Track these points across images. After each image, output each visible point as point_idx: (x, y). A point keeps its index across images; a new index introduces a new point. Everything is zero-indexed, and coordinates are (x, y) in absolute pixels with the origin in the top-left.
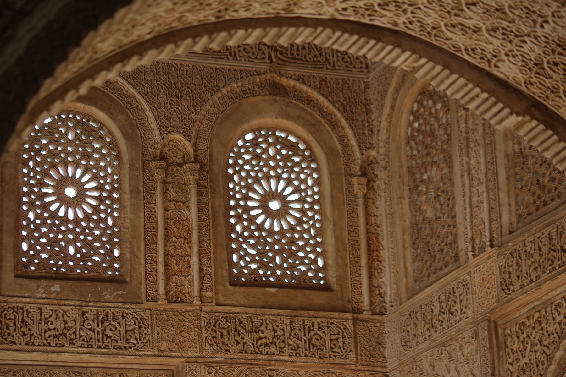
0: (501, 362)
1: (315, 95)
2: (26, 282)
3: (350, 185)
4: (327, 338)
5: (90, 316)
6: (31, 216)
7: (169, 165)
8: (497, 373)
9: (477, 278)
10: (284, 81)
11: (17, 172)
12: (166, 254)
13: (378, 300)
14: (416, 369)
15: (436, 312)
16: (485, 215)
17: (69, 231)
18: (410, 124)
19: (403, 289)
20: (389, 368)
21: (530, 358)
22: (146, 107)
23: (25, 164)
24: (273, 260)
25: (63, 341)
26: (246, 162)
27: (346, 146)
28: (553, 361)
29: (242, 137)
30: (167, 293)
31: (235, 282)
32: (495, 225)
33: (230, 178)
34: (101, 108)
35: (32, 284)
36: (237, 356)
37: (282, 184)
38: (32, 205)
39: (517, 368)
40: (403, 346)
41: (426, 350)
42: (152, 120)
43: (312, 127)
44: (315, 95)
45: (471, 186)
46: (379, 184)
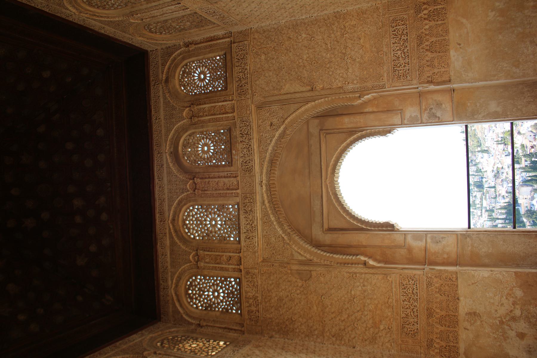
1: (167, 67)
2: (233, 163)
3: (192, 51)
4: (241, 52)
5: (241, 139)
6: (214, 161)
7: (193, 116)
9: (195, 6)
10: (164, 78)
11: (201, 167)
12: (220, 114)
13: (227, 35)
15: (218, 17)
16: (173, 7)
17: (217, 148)
18: (165, 34)
19: (219, 28)
22: (177, 125)
23: (199, 164)
24: (218, 75)
25: (250, 149)
26: (190, 88)
27: (181, 54)
29: (183, 91)
30: (232, 113)
31: (226, 88)
32: (173, 3)
33: (195, 93)
34: (180, 140)
35: (234, 160)
36: (249, 85)
37: (196, 75)
38: (211, 162)
42: (180, 123)
43: (176, 66)
44: (167, 67)
45: (167, 13)
46: (190, 40)
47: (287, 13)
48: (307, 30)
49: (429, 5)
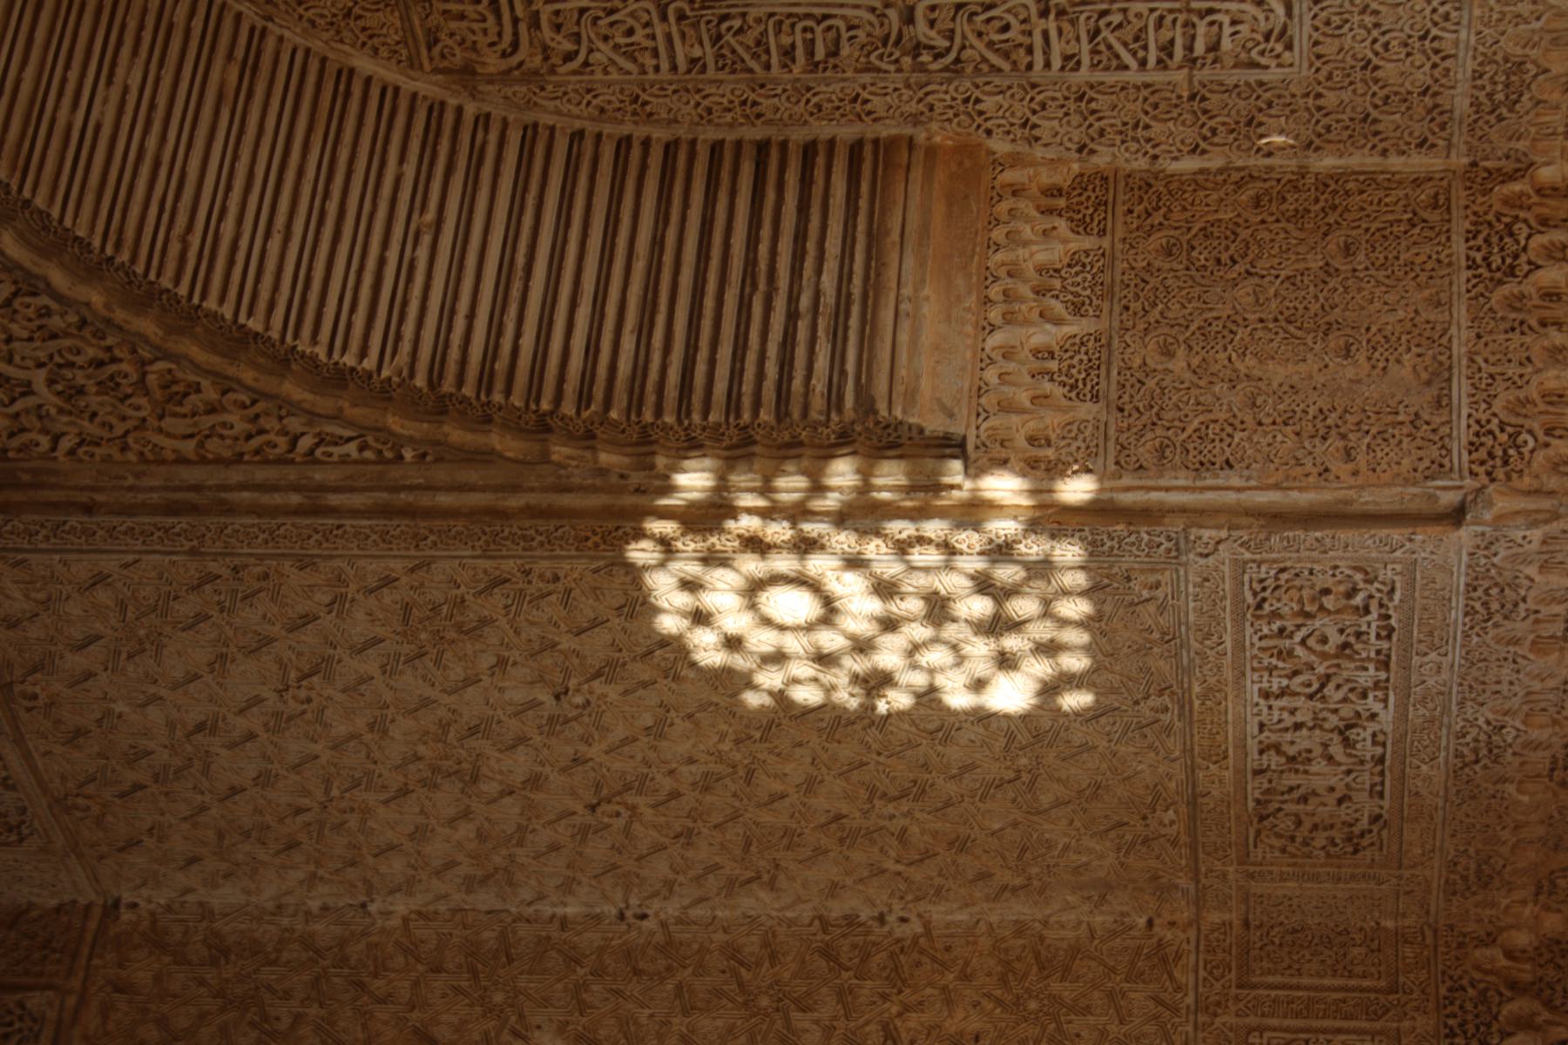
0: (53, 480)
8: (83, 497)
14: (88, 797)
20: (93, 897)
21: (30, 363)
28: (36, 270)
39: (65, 419)
40: (21, 840)
41: (27, 756)
47: (466, 830)
48: (583, 1008)
49: (1548, 1004)
